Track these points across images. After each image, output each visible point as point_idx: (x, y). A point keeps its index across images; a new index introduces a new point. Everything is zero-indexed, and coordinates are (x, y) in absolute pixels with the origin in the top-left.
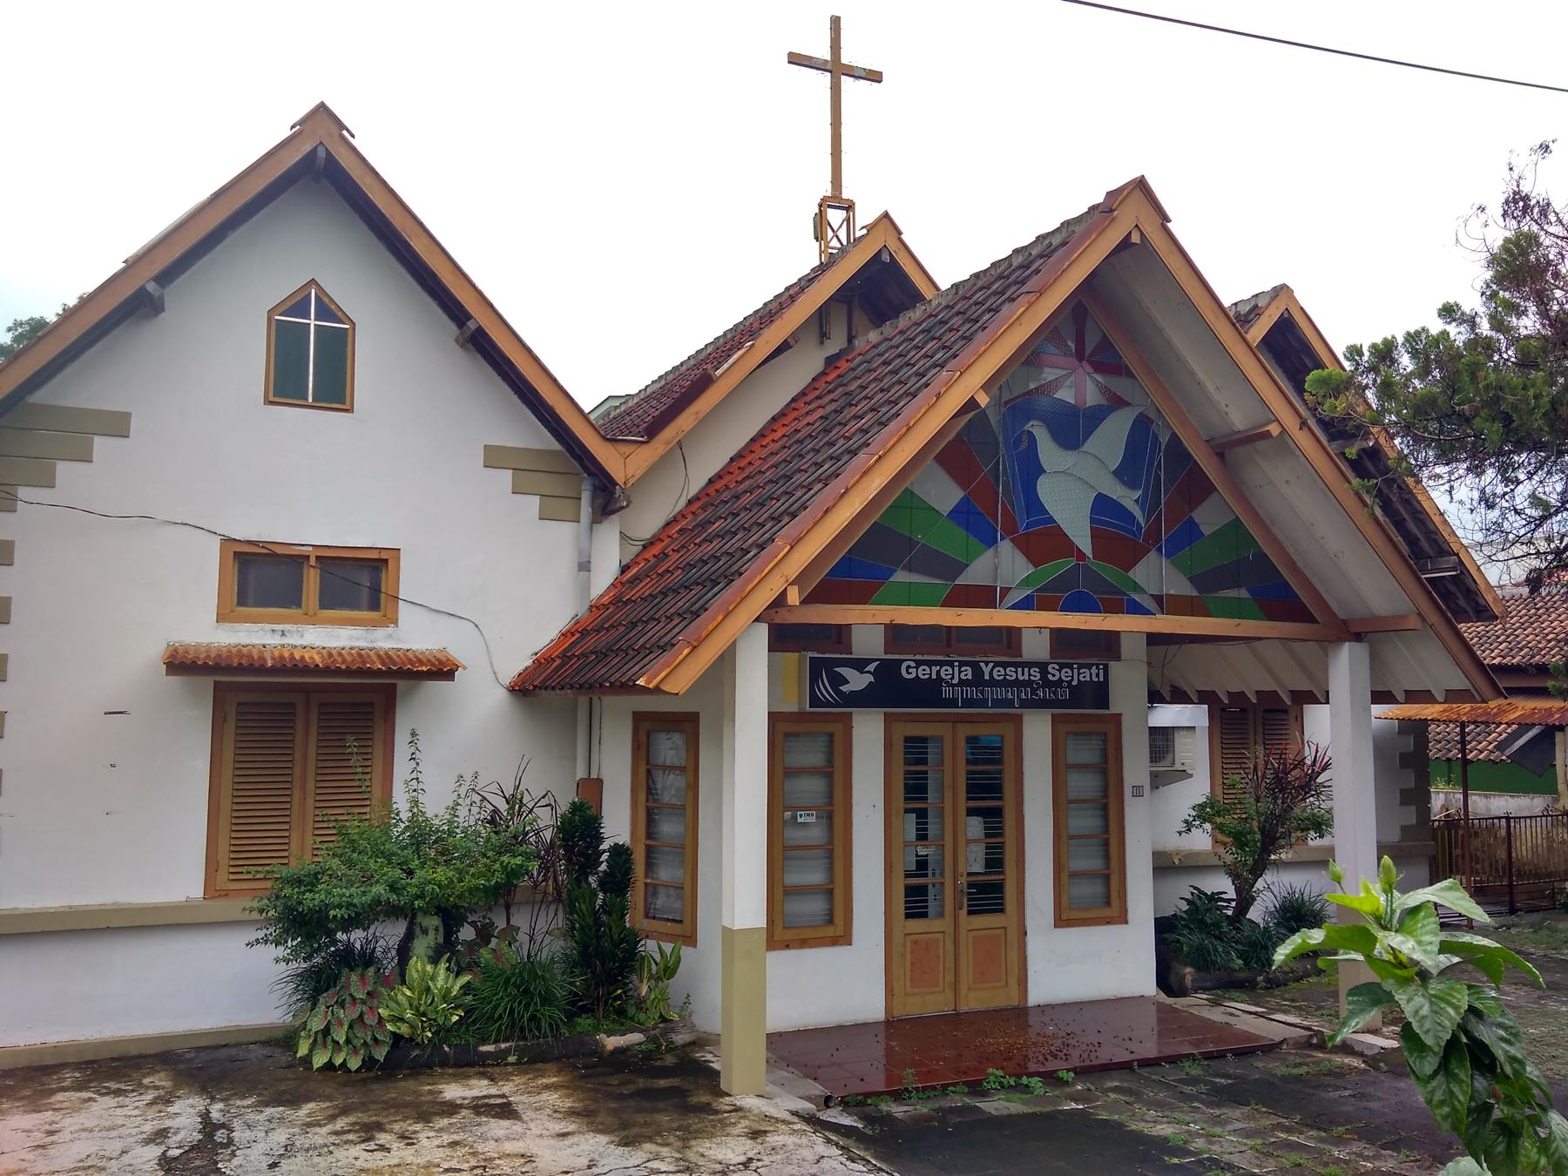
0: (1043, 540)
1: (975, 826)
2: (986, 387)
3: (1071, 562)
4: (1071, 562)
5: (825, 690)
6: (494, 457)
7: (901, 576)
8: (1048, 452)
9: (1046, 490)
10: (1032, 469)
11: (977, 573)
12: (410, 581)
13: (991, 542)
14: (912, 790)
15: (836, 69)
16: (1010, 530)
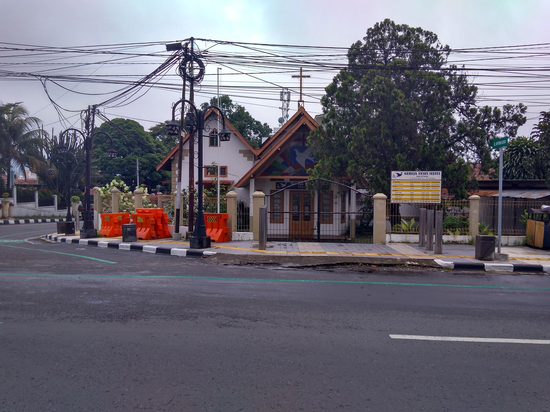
0: (297, 166)
1: (307, 208)
2: (280, 147)
3: (301, 169)
4: (301, 169)
5: (278, 186)
6: (241, 152)
7: (274, 172)
8: (297, 153)
9: (297, 159)
10: (295, 156)
11: (287, 171)
12: (229, 171)
13: (288, 167)
14: (294, 201)
15: (301, 77)
16: (291, 165)
